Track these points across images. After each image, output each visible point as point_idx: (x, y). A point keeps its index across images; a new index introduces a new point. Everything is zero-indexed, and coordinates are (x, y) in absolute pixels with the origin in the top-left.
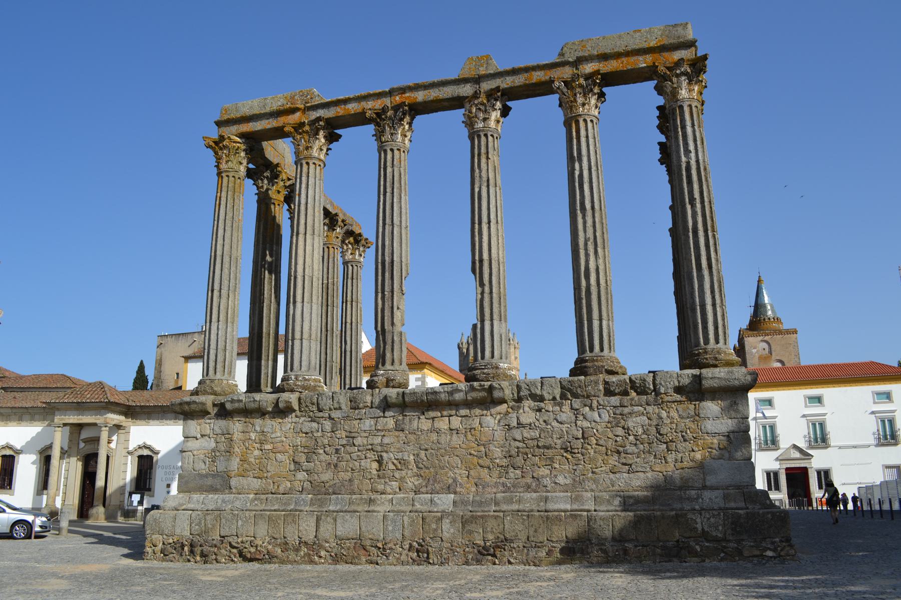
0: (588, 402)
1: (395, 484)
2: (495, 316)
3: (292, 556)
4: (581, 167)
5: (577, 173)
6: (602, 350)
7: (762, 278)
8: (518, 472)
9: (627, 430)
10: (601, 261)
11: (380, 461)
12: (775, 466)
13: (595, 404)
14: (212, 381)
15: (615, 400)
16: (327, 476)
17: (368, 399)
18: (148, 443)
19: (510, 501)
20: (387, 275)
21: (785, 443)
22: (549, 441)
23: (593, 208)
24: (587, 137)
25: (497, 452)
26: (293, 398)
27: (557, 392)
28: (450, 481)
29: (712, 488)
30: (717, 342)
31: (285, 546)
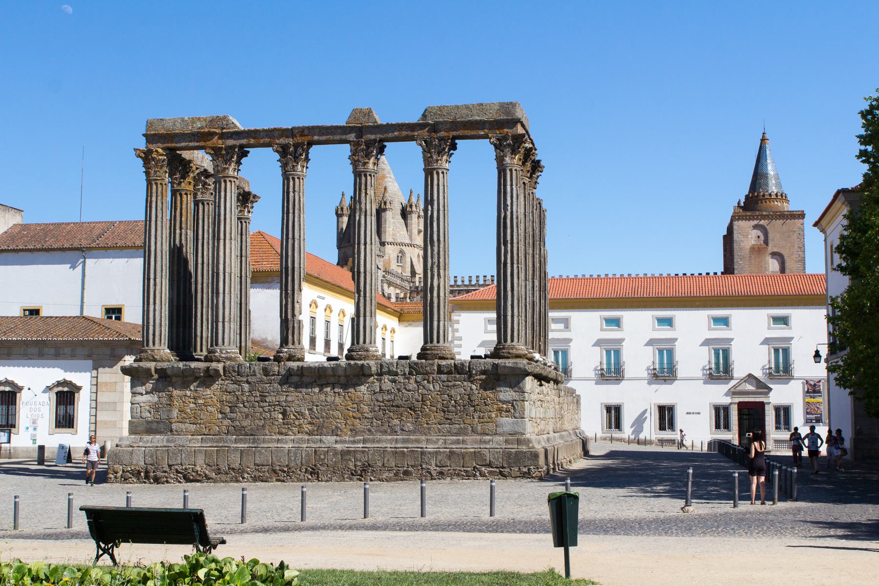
0: (427, 377)
1: (295, 430)
2: (368, 314)
3: (224, 477)
4: (432, 208)
5: (429, 212)
6: (438, 342)
7: (767, 136)
8: (380, 422)
9: (450, 396)
10: (442, 280)
11: (284, 413)
12: (727, 400)
13: (431, 379)
14: (153, 351)
15: (444, 377)
16: (245, 423)
17: (276, 369)
18: (10, 379)
19: (373, 441)
20: (290, 278)
21: (739, 371)
22: (400, 402)
23: (439, 240)
24: (438, 185)
25: (366, 409)
26: (220, 366)
27: (407, 370)
28: (334, 427)
29: (500, 435)
30: (512, 341)
31: (218, 472)
